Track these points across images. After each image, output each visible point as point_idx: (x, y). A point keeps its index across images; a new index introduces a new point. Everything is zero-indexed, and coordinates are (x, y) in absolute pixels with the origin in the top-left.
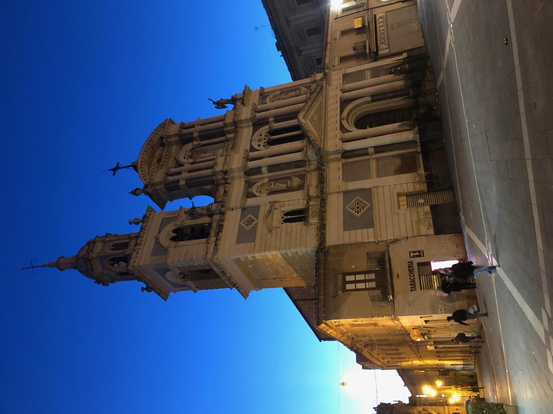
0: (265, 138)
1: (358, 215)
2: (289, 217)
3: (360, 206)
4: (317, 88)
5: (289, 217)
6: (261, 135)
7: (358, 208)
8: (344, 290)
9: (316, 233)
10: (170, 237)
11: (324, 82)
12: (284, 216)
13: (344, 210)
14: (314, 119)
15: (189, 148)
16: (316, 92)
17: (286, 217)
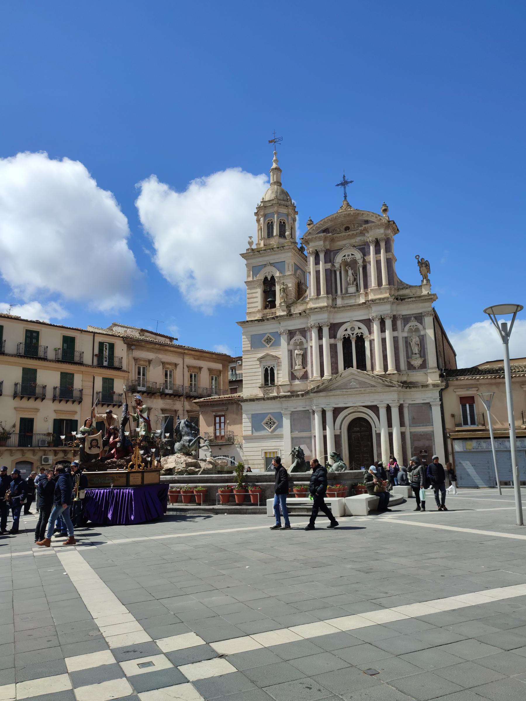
0: (354, 335)
1: (262, 424)
2: (269, 372)
3: (269, 425)
5: (269, 372)
6: (359, 328)
7: (270, 423)
8: (215, 416)
9: (253, 394)
10: (267, 274)
12: (270, 368)
13: (268, 413)
15: (356, 256)
17: (269, 369)
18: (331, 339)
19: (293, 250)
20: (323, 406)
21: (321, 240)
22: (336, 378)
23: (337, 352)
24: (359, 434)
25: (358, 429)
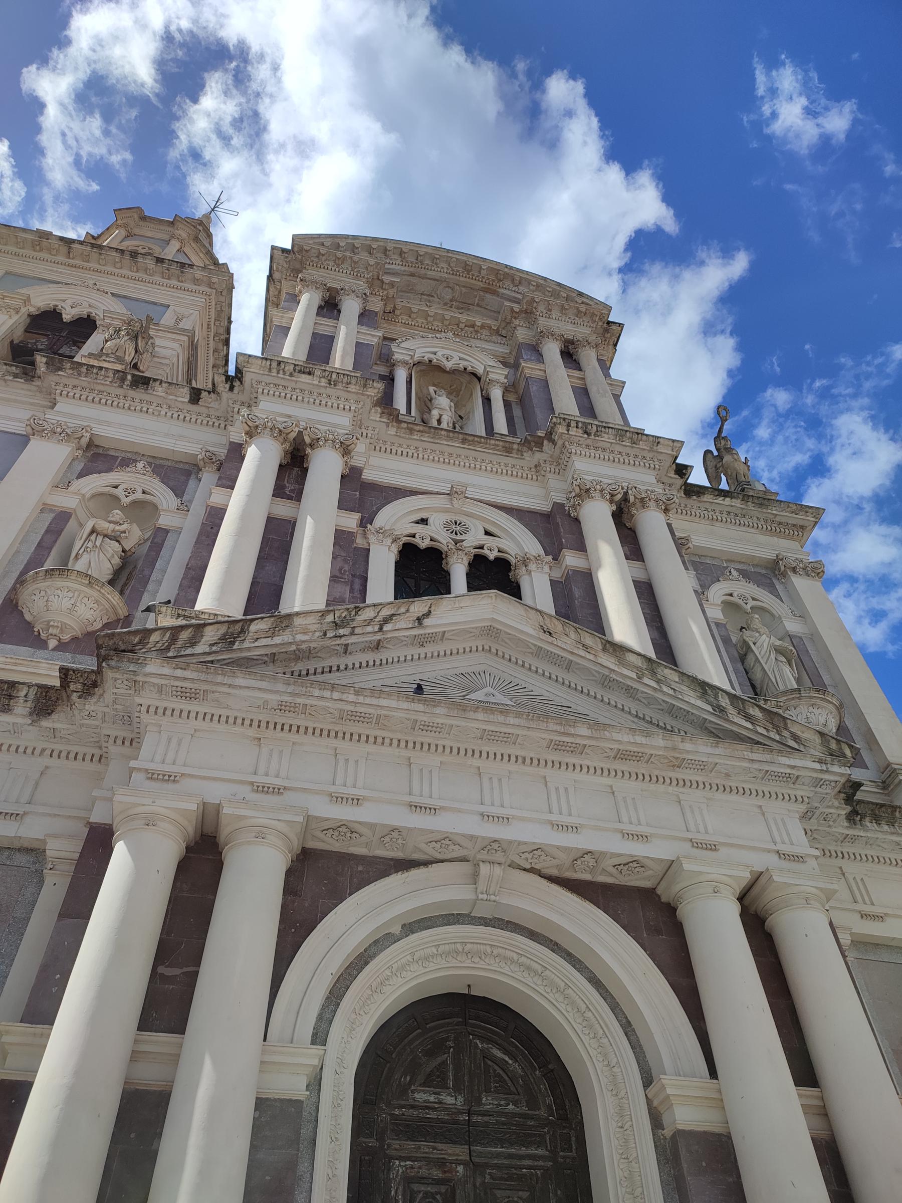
4: (748, 718)
11: (820, 762)
14: (489, 689)
16: (722, 710)
18: (343, 513)
19: (213, 297)
20: (215, 793)
21: (358, 277)
22: (387, 620)
23: (365, 580)
24: (459, 1152)
25: (450, 1100)
